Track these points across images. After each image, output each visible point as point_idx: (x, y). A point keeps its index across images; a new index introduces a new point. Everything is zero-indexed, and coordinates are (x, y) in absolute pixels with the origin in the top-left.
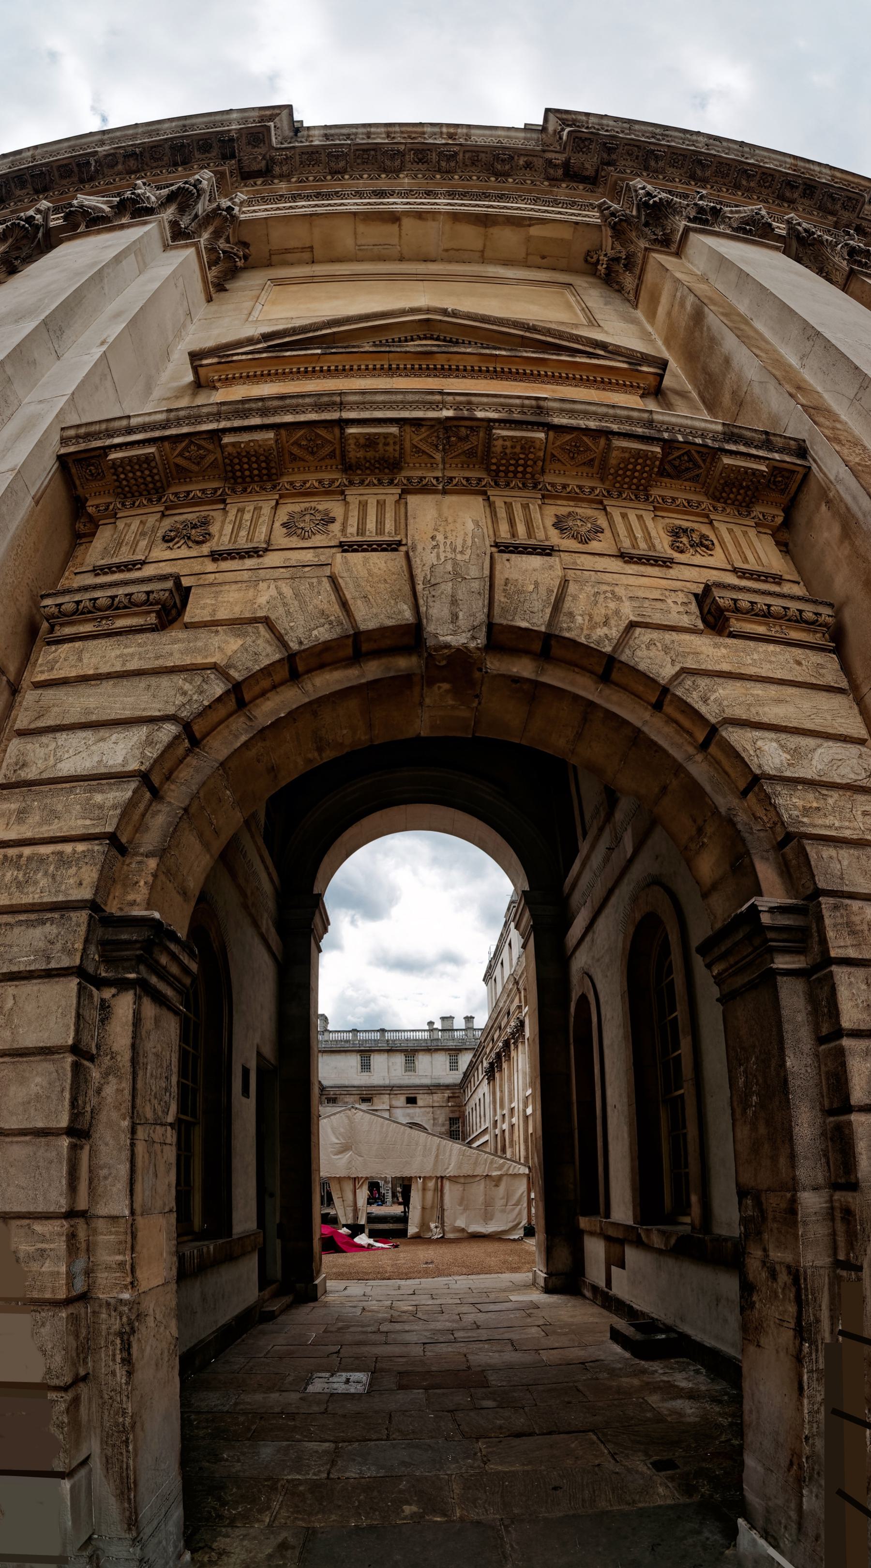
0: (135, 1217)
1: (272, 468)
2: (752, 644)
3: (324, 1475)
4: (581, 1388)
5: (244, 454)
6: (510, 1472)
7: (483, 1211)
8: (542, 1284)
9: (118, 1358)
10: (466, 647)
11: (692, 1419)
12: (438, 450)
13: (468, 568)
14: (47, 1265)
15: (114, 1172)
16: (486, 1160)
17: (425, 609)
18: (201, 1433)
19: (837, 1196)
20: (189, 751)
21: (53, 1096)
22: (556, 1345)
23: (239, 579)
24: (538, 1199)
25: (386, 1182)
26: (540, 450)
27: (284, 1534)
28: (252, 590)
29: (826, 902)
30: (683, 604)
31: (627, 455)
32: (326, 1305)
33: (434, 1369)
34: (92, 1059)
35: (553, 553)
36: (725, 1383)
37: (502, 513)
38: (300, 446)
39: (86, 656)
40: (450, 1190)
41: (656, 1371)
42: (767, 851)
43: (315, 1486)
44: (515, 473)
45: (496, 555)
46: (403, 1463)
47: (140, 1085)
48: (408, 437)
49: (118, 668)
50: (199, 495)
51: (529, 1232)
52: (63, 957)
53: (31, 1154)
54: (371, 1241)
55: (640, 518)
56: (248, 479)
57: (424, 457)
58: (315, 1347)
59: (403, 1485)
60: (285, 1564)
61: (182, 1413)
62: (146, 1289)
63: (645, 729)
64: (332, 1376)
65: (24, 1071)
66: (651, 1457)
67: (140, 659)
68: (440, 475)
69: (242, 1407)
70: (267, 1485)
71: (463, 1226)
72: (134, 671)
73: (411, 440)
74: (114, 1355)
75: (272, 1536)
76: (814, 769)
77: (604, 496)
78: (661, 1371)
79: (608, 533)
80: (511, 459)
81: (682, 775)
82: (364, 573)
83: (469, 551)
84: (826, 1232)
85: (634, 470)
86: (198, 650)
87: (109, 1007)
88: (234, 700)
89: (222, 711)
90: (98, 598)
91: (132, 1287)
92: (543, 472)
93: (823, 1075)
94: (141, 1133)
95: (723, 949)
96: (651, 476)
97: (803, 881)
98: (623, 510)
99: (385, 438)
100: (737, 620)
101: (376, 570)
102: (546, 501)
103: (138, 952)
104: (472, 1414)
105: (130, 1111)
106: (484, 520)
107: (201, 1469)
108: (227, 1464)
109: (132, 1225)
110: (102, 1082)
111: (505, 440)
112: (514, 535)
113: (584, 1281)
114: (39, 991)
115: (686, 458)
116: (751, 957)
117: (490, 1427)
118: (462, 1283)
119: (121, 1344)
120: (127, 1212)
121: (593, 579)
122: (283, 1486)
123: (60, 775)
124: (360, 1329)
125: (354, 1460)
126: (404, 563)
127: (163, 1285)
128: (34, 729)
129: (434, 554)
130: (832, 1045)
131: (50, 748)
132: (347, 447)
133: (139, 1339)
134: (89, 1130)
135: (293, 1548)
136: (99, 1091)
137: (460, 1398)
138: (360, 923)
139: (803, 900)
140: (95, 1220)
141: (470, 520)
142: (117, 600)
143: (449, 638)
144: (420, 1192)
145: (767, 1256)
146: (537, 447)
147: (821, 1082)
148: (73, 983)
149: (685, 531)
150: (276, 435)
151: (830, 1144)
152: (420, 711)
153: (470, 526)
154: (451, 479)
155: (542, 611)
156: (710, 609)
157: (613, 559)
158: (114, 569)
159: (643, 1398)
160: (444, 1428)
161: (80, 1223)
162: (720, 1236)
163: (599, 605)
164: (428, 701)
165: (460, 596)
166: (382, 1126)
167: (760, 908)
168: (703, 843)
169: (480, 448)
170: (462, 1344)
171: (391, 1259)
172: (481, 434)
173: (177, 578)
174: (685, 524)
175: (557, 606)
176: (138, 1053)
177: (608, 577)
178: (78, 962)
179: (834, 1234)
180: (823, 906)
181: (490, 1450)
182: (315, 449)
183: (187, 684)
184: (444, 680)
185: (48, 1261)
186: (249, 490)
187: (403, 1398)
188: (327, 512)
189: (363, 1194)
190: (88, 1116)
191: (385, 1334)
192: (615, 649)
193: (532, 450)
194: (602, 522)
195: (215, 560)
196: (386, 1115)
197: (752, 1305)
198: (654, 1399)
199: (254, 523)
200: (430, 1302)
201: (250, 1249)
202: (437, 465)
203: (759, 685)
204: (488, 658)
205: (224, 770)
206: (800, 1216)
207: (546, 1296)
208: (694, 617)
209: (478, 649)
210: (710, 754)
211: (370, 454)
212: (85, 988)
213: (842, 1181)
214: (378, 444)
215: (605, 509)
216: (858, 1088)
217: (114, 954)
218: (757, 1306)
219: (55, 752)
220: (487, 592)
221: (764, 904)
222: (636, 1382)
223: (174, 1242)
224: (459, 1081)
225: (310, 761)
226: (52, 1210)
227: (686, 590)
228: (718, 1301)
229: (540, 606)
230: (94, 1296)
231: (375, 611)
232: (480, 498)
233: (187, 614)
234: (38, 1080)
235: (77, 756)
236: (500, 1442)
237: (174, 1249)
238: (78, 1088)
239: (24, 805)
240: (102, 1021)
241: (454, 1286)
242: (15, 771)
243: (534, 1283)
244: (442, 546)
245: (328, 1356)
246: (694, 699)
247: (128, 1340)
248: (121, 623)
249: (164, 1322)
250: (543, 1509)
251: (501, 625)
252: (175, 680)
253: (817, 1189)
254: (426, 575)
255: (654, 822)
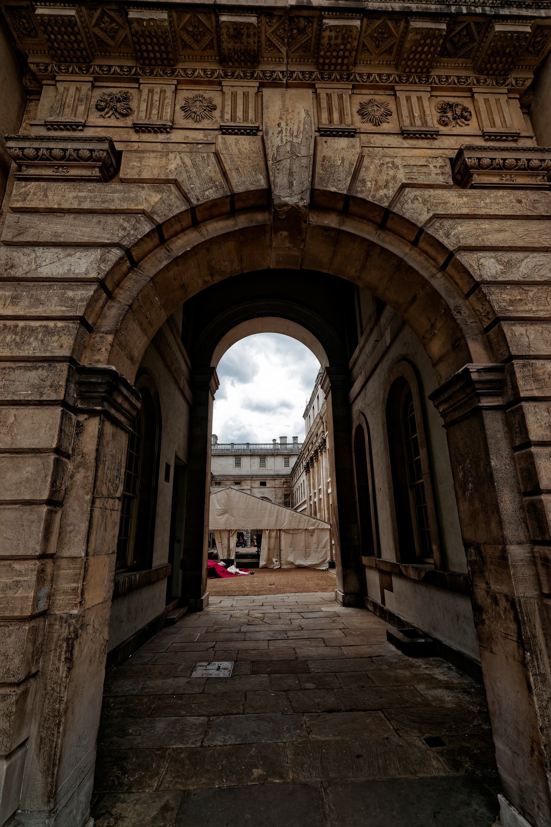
0: (89, 557)
1: (170, 52)
2: (486, 192)
3: (199, 744)
4: (370, 676)
5: (147, 33)
6: (326, 741)
7: (304, 551)
8: (341, 600)
9: (63, 657)
10: (297, 206)
11: (450, 705)
12: (283, 43)
13: (300, 149)
14: (20, 592)
15: (77, 528)
16: (305, 520)
17: (273, 178)
18: (116, 713)
19: (536, 548)
20: (130, 270)
21: (39, 480)
22: (352, 643)
23: (155, 149)
24: (336, 544)
25: (248, 533)
26: (355, 39)
27: (167, 797)
28: (164, 159)
29: (517, 363)
30: (441, 167)
31: (419, 37)
32: (208, 613)
33: (274, 659)
34: (68, 457)
35: (356, 135)
36: (471, 679)
37: (324, 104)
38: (188, 32)
39: (50, 194)
40: (285, 538)
41: (420, 666)
42: (477, 335)
43: (192, 753)
44: (336, 64)
45: (318, 138)
46: (255, 733)
47: (100, 473)
48: (264, 28)
49: (75, 206)
50: (119, 71)
51: (332, 565)
52: (52, 394)
53: (19, 516)
54: (237, 570)
55: (419, 99)
56: (153, 62)
57: (275, 51)
58: (199, 644)
59: (253, 751)
60: (165, 825)
61: (103, 697)
62: (89, 607)
63: (406, 259)
64: (209, 664)
65: (19, 463)
66: (423, 734)
67: (91, 201)
68: (285, 69)
69: (146, 690)
70: (159, 754)
71: (292, 561)
72: (87, 209)
73: (266, 32)
74: (60, 656)
75: (158, 800)
76: (521, 274)
77: (396, 82)
78: (424, 666)
79: (395, 115)
80: (335, 50)
81: (427, 287)
82: (236, 151)
83: (301, 135)
84: (531, 573)
85: (422, 52)
86: (129, 199)
87: (82, 426)
88: (157, 237)
89: (150, 244)
90: (53, 149)
91: (81, 605)
92: (355, 64)
93: (518, 472)
94: (98, 503)
95: (446, 396)
96: (434, 56)
97: (501, 351)
98: (407, 94)
99: (248, 28)
100: (478, 175)
101: (243, 150)
102: (356, 91)
103: (103, 394)
104: (299, 693)
105: (92, 490)
106: (312, 110)
107: (112, 743)
108: (132, 737)
109: (86, 563)
110: (74, 471)
111: (331, 31)
112: (331, 121)
113: (367, 599)
114: (34, 413)
115: (465, 33)
116: (465, 400)
117: (312, 703)
118: (292, 598)
119: (67, 647)
120: (83, 554)
121: (380, 153)
122: (169, 754)
123: (41, 276)
124: (228, 630)
125: (220, 730)
126: (260, 145)
127: (102, 602)
128: (17, 242)
129: (279, 138)
130: (524, 451)
131: (31, 257)
132: (221, 37)
133: (80, 643)
134: (63, 501)
135: (173, 809)
136: (72, 477)
137: (291, 681)
138: (236, 384)
139: (501, 363)
140: (60, 560)
141: (303, 110)
142: (68, 153)
143: (287, 199)
144: (267, 539)
145: (490, 588)
146: (354, 36)
147: (517, 475)
148: (59, 410)
149: (451, 106)
150: (170, 16)
151: (527, 514)
152: (270, 251)
153: (303, 115)
154: (292, 73)
155: (345, 179)
156: (459, 169)
157: (396, 136)
158: (62, 127)
159: (413, 686)
160: (281, 704)
161: (49, 562)
162: (455, 572)
163: (383, 173)
164: (274, 244)
165: (294, 170)
166: (246, 498)
167: (471, 370)
168: (435, 334)
169: (313, 39)
170: (292, 641)
171: (249, 582)
172: (315, 26)
173: (111, 143)
174: (452, 100)
175: (355, 176)
176: (100, 454)
177: (390, 152)
178: (62, 397)
179: (537, 575)
180: (515, 366)
181: (312, 722)
182: (199, 38)
183: (126, 223)
184: (284, 229)
185: (21, 589)
186: (155, 73)
187: (254, 680)
188: (210, 101)
189: (234, 540)
190: (63, 493)
191: (244, 634)
192: (390, 205)
193: (350, 40)
194: (392, 107)
195: (137, 132)
196: (249, 492)
197: (483, 621)
198: (421, 687)
199: (161, 107)
200: (272, 611)
201: (162, 576)
202: (283, 59)
203: (487, 221)
204: (310, 215)
205: (153, 283)
206: (510, 561)
207: (344, 608)
208: (447, 176)
209: (304, 206)
210: (447, 273)
211: (238, 46)
212: (66, 413)
213: (539, 539)
214: (243, 35)
215: (395, 95)
216: (545, 478)
217: (87, 394)
218: (486, 622)
219: (35, 260)
220: (311, 166)
221: (474, 367)
222: (407, 673)
223: (113, 573)
224: (290, 473)
225: (206, 282)
226: (29, 553)
227: (444, 156)
228: (458, 617)
229: (344, 176)
230: (52, 613)
231: (243, 179)
232: (310, 91)
233: (121, 172)
234: (29, 469)
235: (53, 265)
236: (318, 716)
237: (113, 578)
238: (57, 474)
239: (15, 293)
240: (77, 434)
241: (287, 600)
242: (6, 270)
243: (336, 599)
244: (284, 132)
245: (207, 650)
246: (440, 236)
247: (72, 643)
248: (73, 172)
249: (100, 629)
250: (351, 774)
251: (319, 190)
252: (117, 219)
253: (520, 544)
254: (274, 153)
255: (404, 323)
